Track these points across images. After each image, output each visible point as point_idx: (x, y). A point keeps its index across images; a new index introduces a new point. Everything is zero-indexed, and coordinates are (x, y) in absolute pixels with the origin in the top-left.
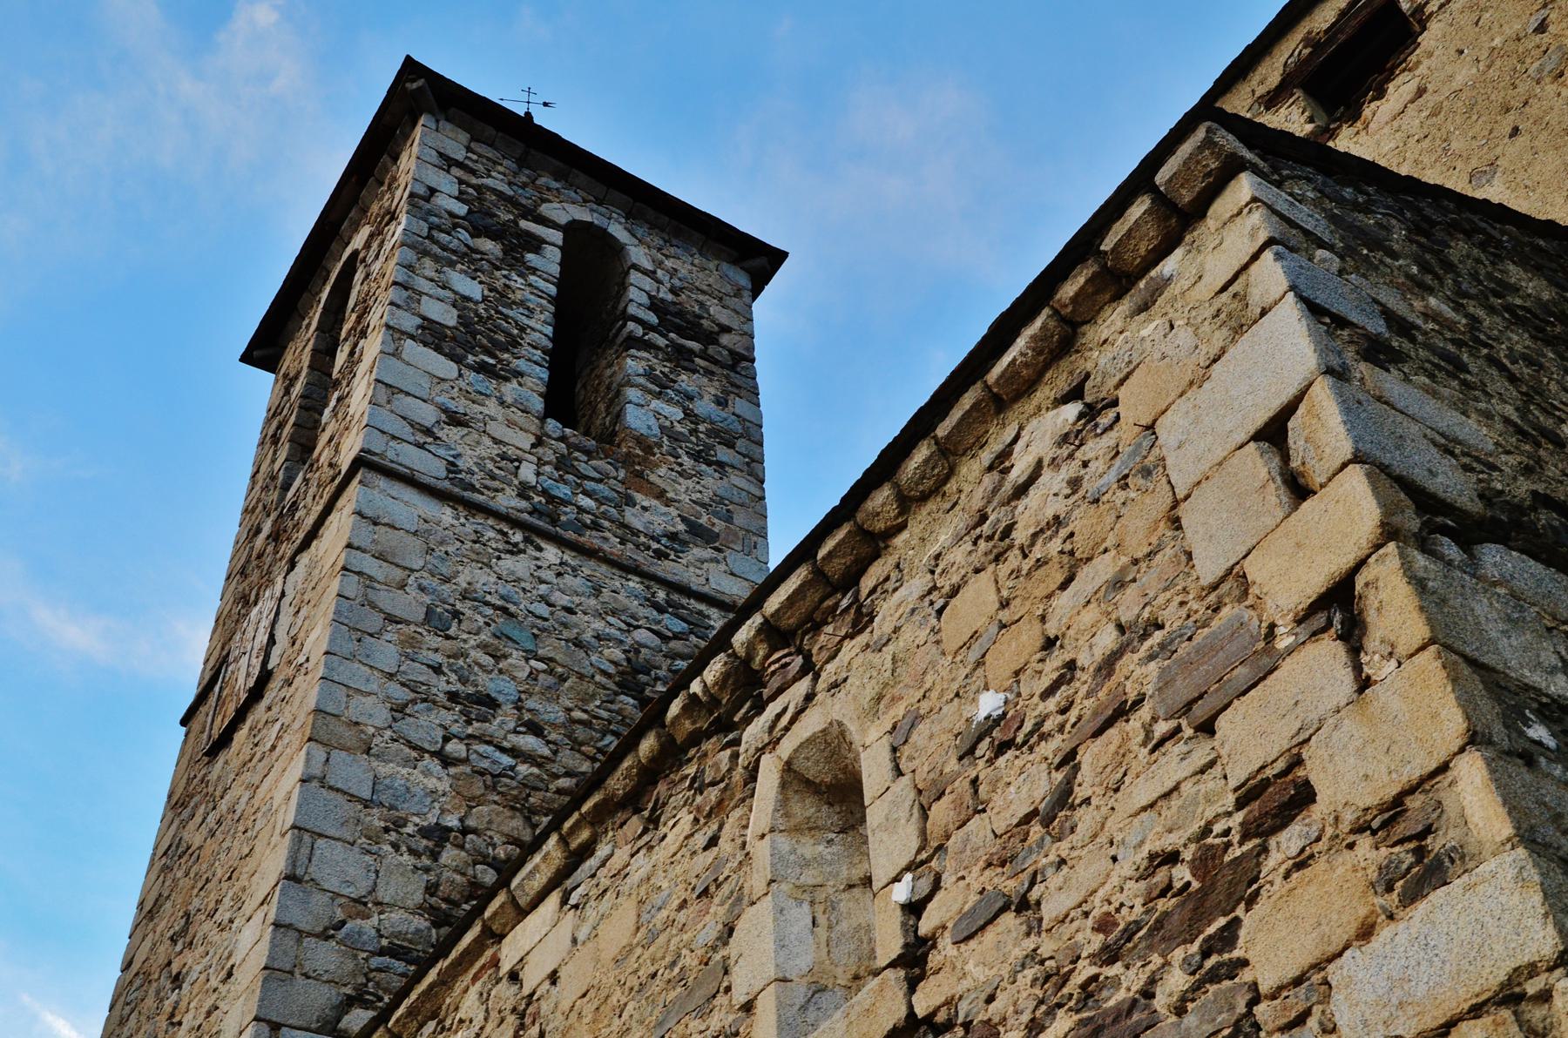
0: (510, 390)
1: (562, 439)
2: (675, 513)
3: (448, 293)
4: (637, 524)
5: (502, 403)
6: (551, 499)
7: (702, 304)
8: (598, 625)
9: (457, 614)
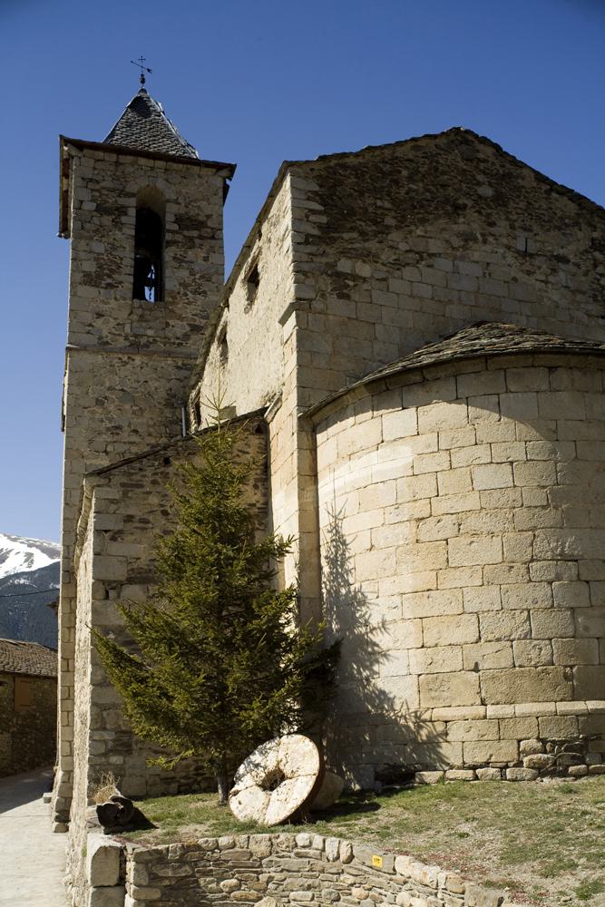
0: (119, 292)
1: (141, 307)
2: (185, 323)
3: (92, 255)
4: (170, 335)
5: (116, 299)
6: (136, 336)
7: (199, 207)
8: (157, 384)
9: (106, 398)
